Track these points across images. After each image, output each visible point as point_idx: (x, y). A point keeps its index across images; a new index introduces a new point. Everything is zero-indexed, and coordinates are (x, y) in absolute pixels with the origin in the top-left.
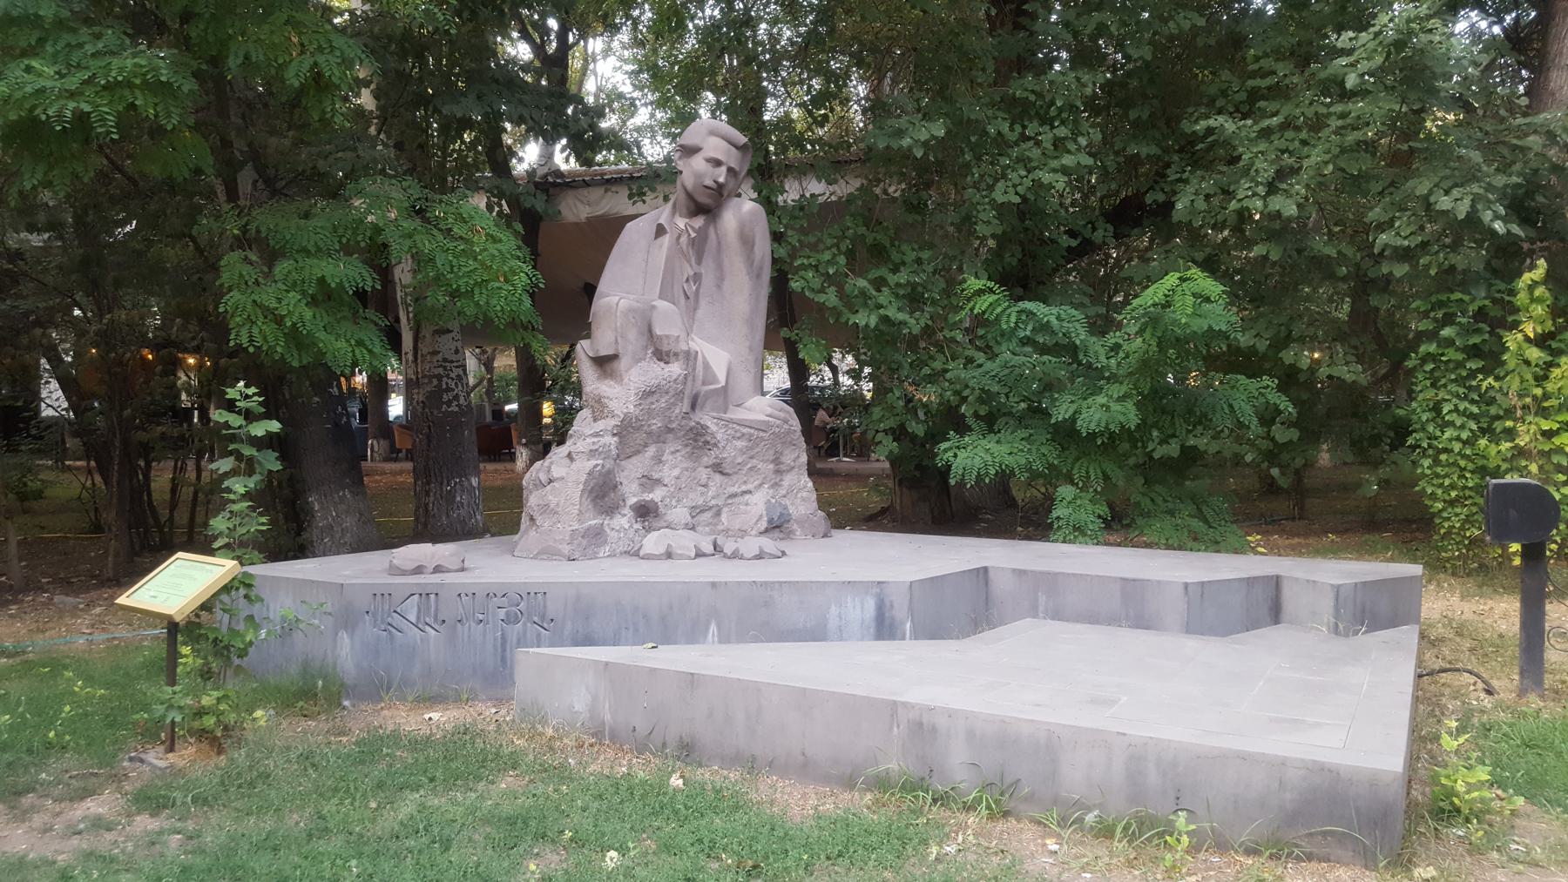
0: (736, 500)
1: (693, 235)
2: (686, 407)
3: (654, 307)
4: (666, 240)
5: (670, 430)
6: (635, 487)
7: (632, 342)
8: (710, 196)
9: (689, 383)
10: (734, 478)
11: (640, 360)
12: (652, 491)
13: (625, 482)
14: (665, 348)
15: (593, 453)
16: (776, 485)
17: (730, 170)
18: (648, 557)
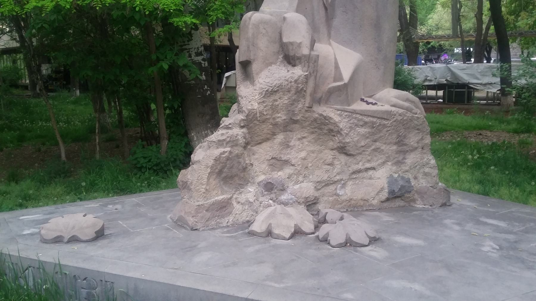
0: (360, 174)
5: (296, 122)
6: (264, 166)
9: (311, 84)
10: (359, 158)
11: (270, 64)
12: (281, 169)
13: (256, 163)
14: (291, 54)
15: (220, 143)
16: (399, 163)
18: (252, 234)
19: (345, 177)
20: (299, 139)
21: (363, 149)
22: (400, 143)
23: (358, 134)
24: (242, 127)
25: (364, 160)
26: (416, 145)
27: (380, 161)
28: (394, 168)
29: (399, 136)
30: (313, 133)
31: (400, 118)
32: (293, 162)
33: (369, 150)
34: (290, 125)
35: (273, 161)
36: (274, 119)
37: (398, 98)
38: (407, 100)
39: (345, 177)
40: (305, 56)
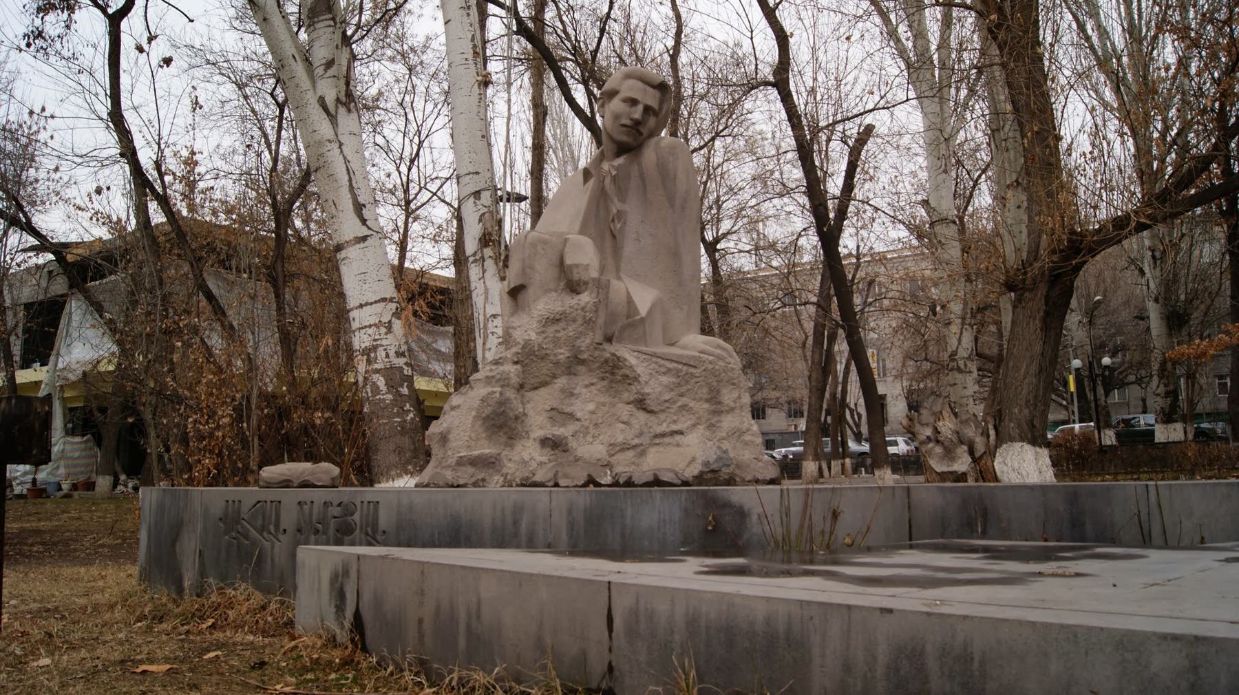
0: (667, 440)
1: (614, 173)
2: (599, 337)
3: (566, 240)
4: (591, 182)
5: (583, 362)
7: (543, 271)
8: (628, 134)
10: (662, 416)
12: (563, 425)
13: (531, 413)
14: (576, 277)
15: (489, 380)
16: (711, 427)
17: (647, 109)
19: (645, 440)
20: (586, 386)
21: (667, 405)
22: (714, 398)
23: (660, 384)
24: (516, 363)
25: (669, 420)
26: (732, 404)
27: (689, 423)
28: (708, 433)
29: (711, 391)
30: (603, 379)
31: (710, 367)
32: (579, 415)
33: (675, 407)
34: (576, 362)
35: (553, 413)
36: (555, 355)
37: (705, 343)
38: (719, 347)
39: (645, 440)
40: (594, 279)
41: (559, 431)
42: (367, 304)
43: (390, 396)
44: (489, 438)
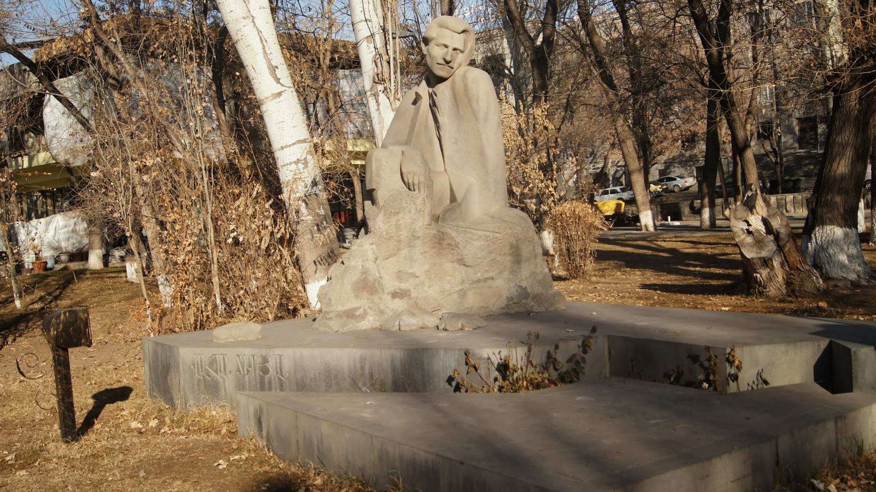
28: (511, 277)
32: (418, 274)
41: (404, 286)
42: (286, 146)
43: (310, 217)
44: (357, 297)
